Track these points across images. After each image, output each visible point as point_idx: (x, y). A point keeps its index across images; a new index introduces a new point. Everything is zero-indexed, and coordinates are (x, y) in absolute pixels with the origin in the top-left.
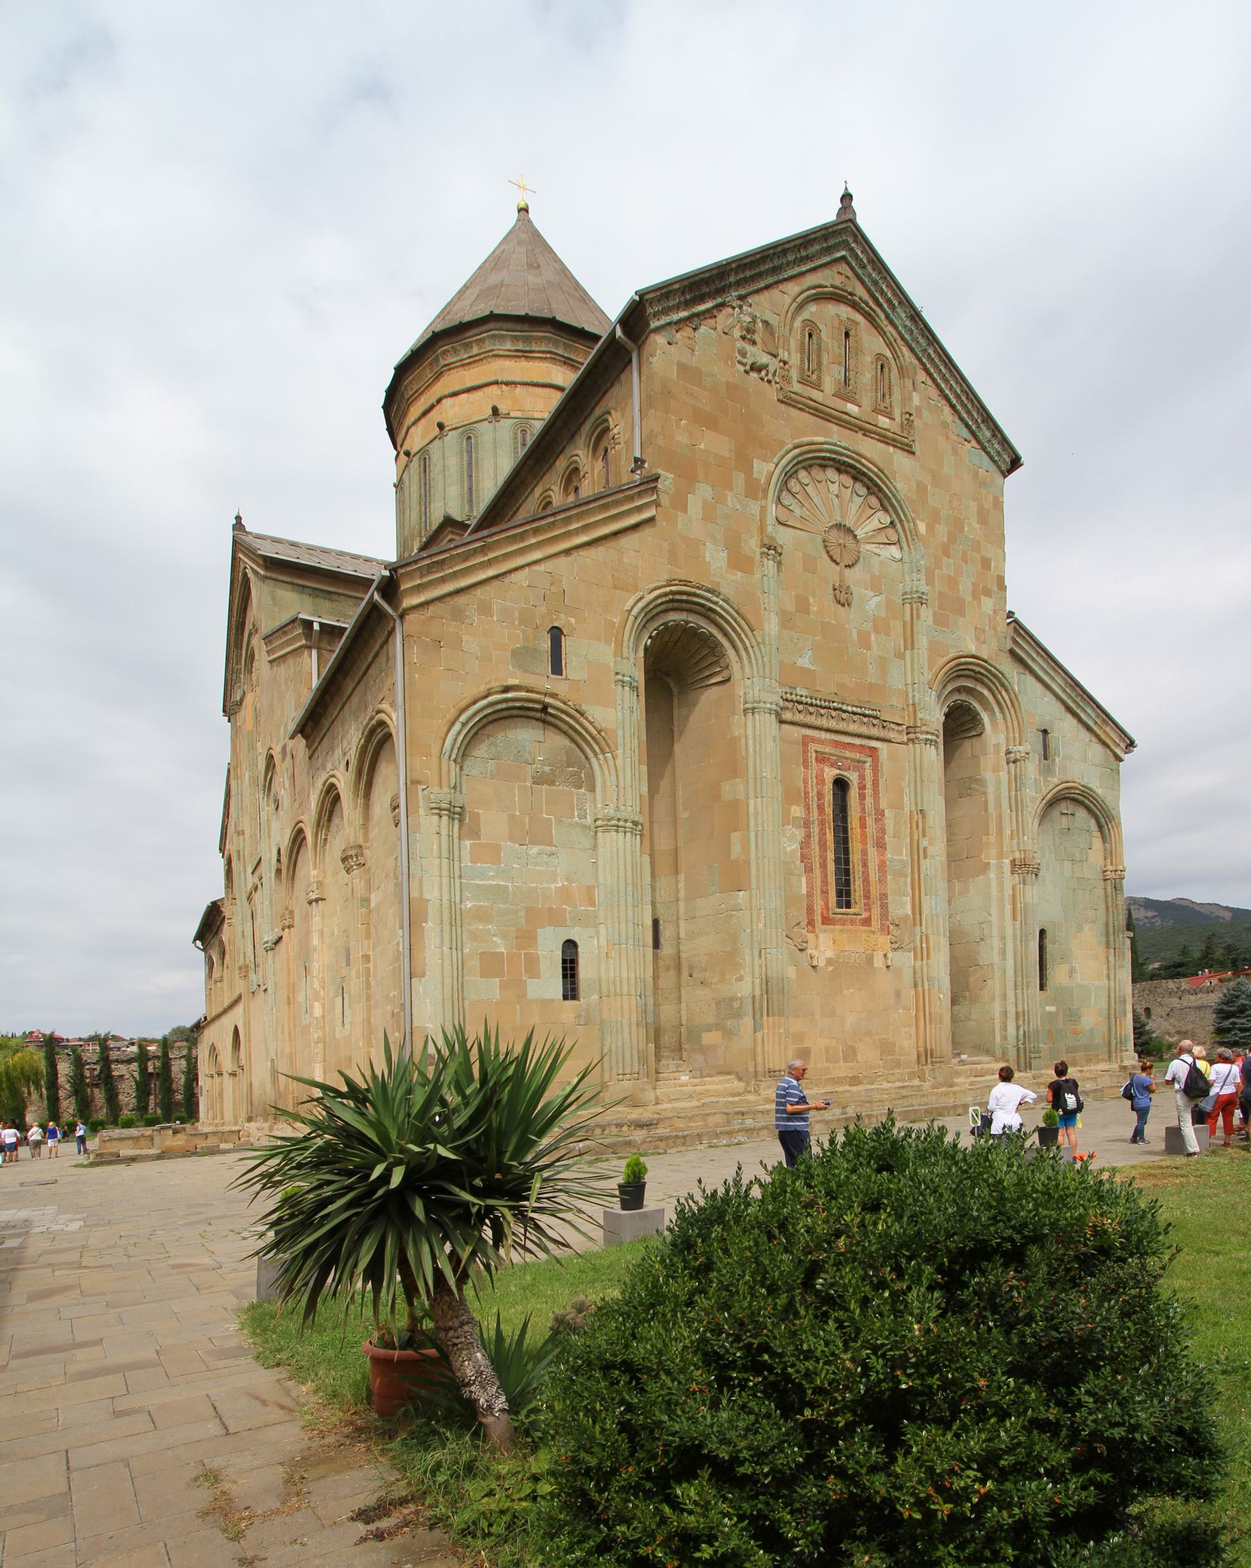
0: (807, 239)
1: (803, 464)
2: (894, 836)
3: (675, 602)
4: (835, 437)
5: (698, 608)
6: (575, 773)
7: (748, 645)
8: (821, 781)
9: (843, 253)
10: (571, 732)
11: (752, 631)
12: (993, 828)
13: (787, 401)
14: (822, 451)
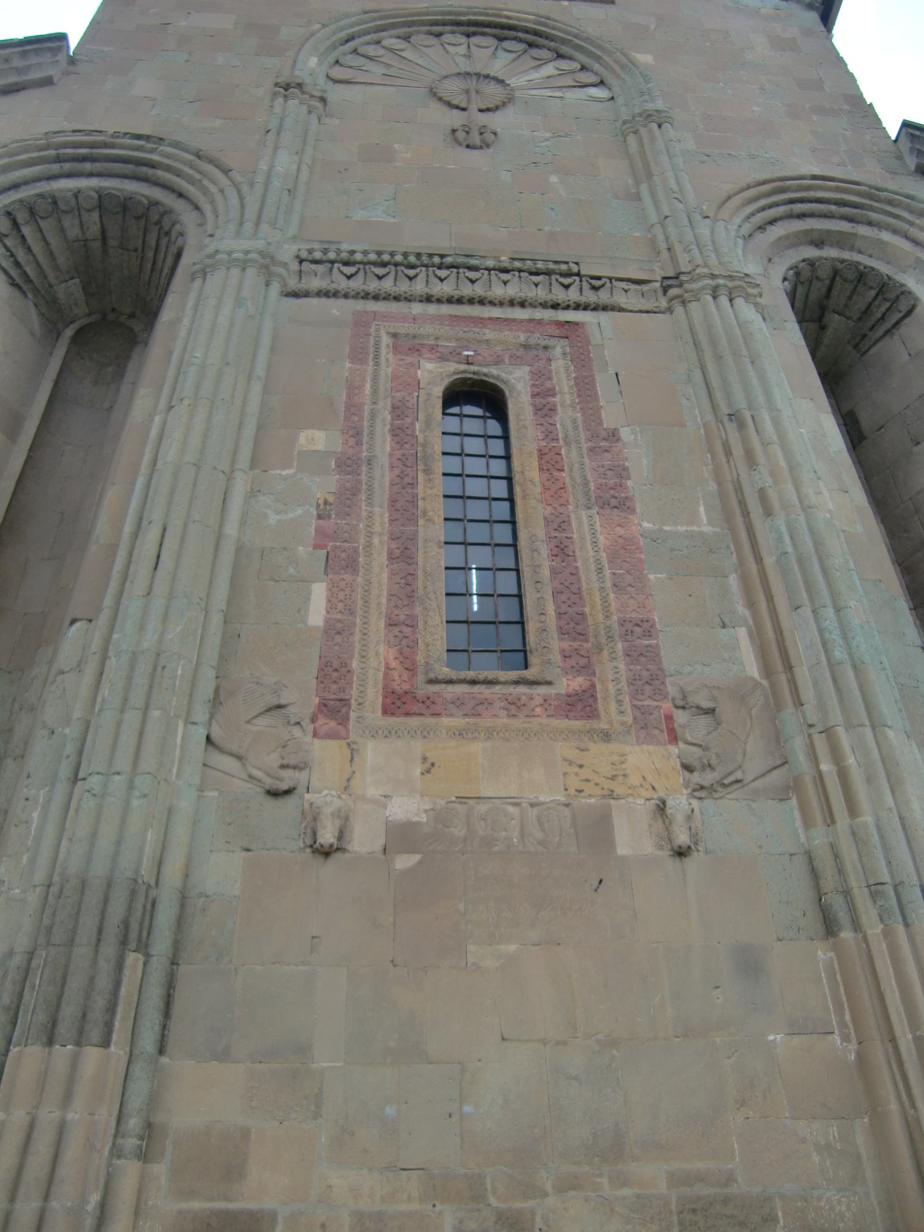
1: (393, 32)
7: (213, 189)
11: (226, 172)
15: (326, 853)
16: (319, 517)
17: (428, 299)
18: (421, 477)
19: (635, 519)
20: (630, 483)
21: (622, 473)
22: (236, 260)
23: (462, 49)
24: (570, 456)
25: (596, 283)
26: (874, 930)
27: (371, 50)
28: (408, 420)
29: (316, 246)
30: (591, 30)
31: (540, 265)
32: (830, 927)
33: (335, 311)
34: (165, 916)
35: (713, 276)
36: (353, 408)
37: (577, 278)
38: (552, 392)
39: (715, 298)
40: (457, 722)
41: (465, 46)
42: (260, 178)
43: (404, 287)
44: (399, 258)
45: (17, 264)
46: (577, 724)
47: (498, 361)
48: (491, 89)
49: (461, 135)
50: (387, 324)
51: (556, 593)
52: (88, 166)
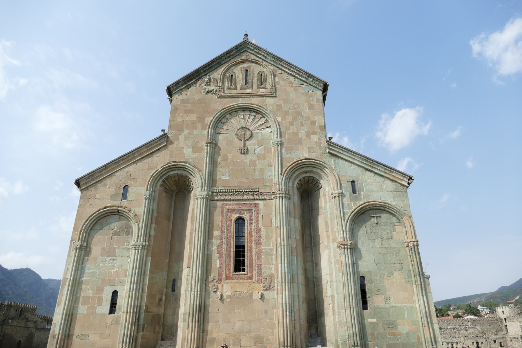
0: (228, 52)
2: (266, 238)
4: (241, 101)
5: (180, 168)
6: (128, 231)
8: (229, 220)
9: (245, 50)
14: (235, 107)
16: (218, 248)
19: (261, 246)
20: (262, 239)
23: (242, 117)
25: (262, 193)
28: (230, 228)
30: (269, 108)
35: (280, 194)
36: (222, 226)
38: (252, 220)
40: (236, 281)
43: (230, 197)
45: (166, 188)
46: (250, 281)
50: (227, 206)
52: (175, 169)
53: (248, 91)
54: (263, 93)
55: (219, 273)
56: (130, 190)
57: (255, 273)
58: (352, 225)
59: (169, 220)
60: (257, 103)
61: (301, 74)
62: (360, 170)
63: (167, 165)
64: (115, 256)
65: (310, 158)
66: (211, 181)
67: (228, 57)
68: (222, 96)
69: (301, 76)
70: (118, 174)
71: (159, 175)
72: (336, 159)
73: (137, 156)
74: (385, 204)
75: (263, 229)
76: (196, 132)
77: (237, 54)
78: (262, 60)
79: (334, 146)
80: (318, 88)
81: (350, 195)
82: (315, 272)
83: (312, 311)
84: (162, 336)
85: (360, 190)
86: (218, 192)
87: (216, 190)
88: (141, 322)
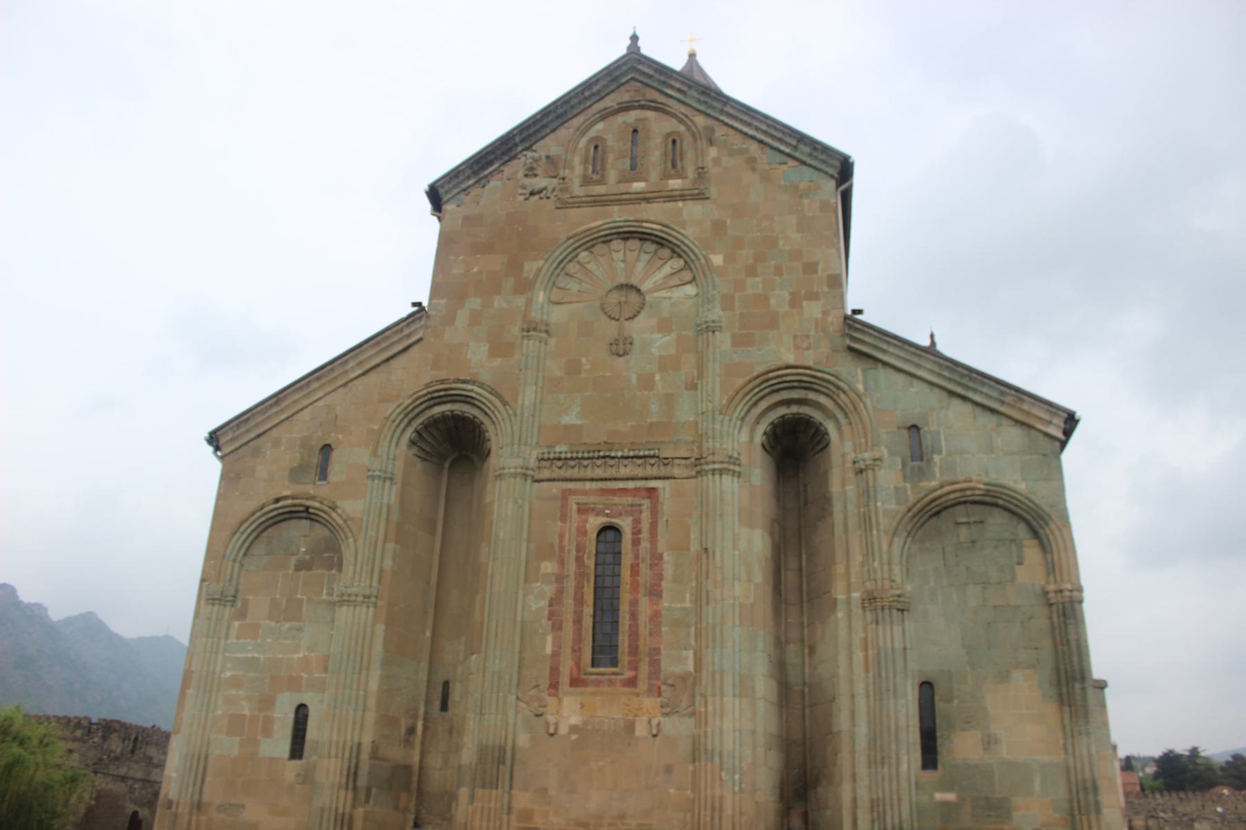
1: (584, 247)
3: (436, 399)
4: (619, 216)
7: (500, 418)
8: (582, 532)
10: (328, 524)
11: (505, 404)
12: (839, 555)
13: (563, 205)
15: (552, 735)
17: (592, 480)
18: (586, 584)
21: (660, 577)
22: (512, 474)
23: (620, 255)
24: (644, 569)
25: (666, 462)
26: (703, 763)
27: (572, 268)
29: (545, 450)
30: (690, 232)
31: (641, 453)
32: (694, 760)
33: (554, 490)
34: (509, 754)
36: (562, 548)
37: (657, 459)
38: (639, 532)
39: (713, 474)
41: (622, 252)
42: (519, 412)
44: (580, 455)
47: (620, 515)
48: (633, 297)
49: (614, 347)
51: (630, 636)
52: (445, 399)
53: (639, 186)
54: (676, 190)
55: (551, 668)
56: (335, 455)
57: (644, 669)
58: (906, 548)
59: (432, 532)
60: (660, 218)
61: (779, 135)
62: (934, 397)
63: (423, 389)
64: (299, 620)
65: (798, 363)
66: (536, 429)
67: (586, 99)
68: (567, 203)
69: (780, 140)
70: (305, 415)
71: (406, 415)
72: (869, 364)
73: (353, 369)
74: (1000, 489)
75: (668, 555)
76: (499, 302)
77: (609, 90)
78: (675, 102)
79: (863, 332)
80: (826, 173)
81: (904, 464)
82: (807, 670)
83: (796, 771)
84: (417, 818)
85: (933, 452)
86: (555, 459)
87: (549, 453)
88: (362, 781)
